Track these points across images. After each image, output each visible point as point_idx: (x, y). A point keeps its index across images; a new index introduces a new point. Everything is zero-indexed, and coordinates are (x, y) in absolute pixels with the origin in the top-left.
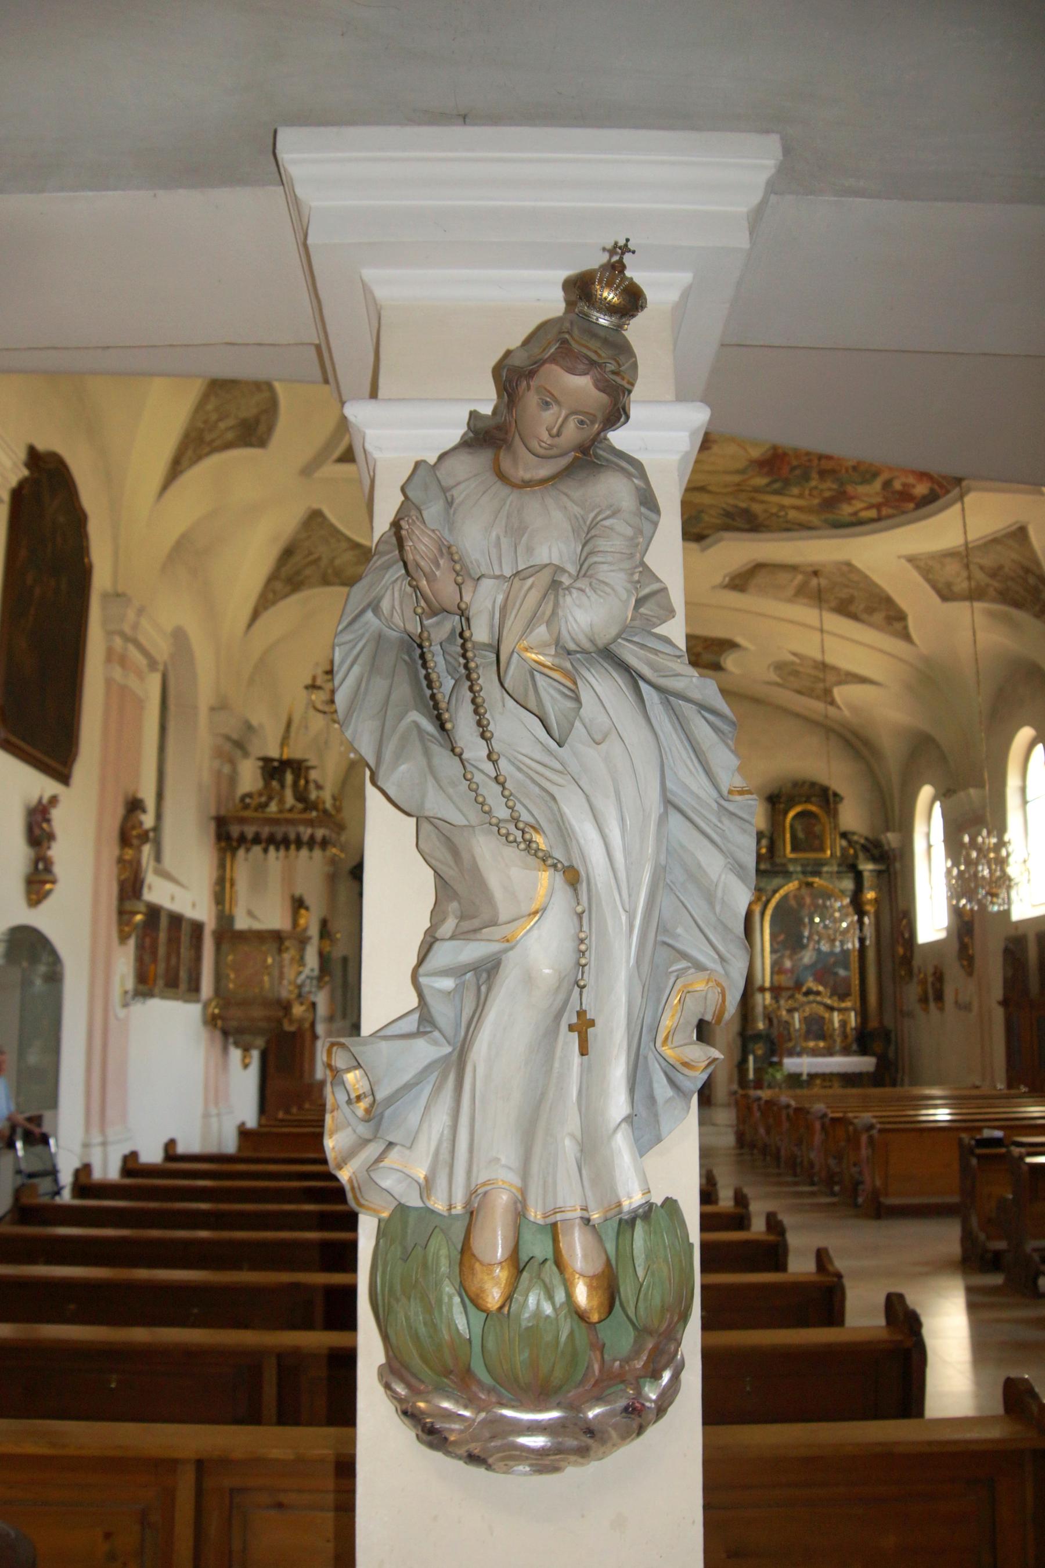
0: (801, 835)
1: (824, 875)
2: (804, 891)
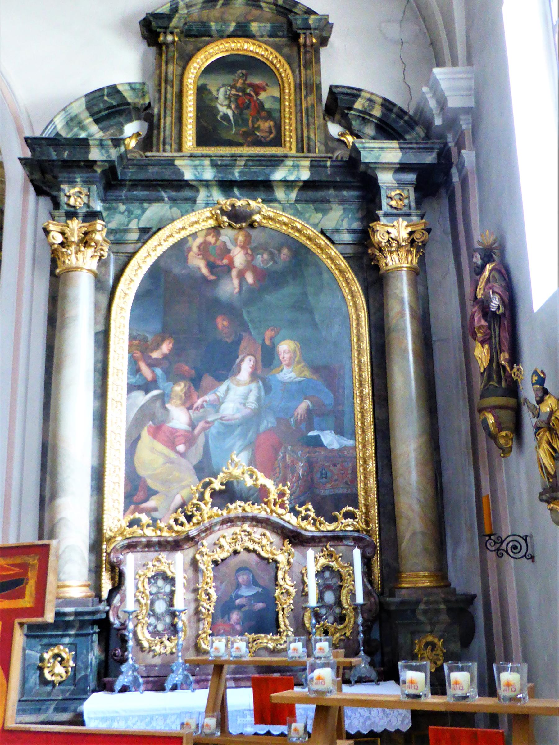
0: (224, 109)
1: (280, 194)
2: (227, 235)
